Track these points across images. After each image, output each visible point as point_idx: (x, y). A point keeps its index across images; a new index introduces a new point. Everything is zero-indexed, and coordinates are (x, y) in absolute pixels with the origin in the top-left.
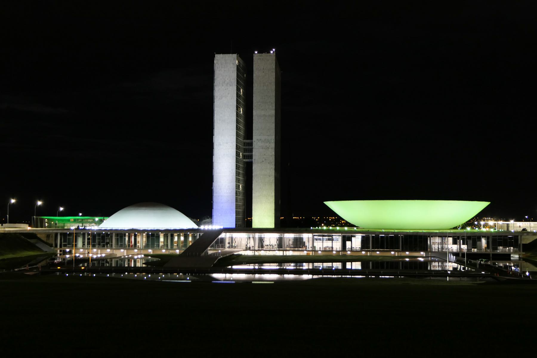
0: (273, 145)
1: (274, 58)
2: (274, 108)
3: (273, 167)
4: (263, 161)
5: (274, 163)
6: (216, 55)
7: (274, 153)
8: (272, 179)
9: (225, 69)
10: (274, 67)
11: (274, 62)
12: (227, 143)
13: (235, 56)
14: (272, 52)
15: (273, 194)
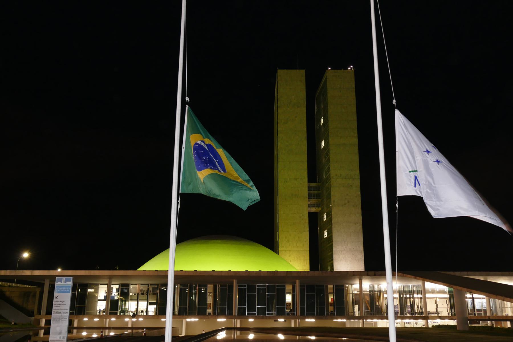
0: (357, 182)
1: (353, 74)
2: (356, 135)
3: (360, 211)
4: (345, 204)
5: (360, 207)
6: (279, 71)
7: (359, 193)
8: (359, 227)
9: (290, 88)
10: (354, 86)
11: (354, 80)
12: (295, 179)
13: (303, 72)
14: (349, 68)
15: (362, 248)
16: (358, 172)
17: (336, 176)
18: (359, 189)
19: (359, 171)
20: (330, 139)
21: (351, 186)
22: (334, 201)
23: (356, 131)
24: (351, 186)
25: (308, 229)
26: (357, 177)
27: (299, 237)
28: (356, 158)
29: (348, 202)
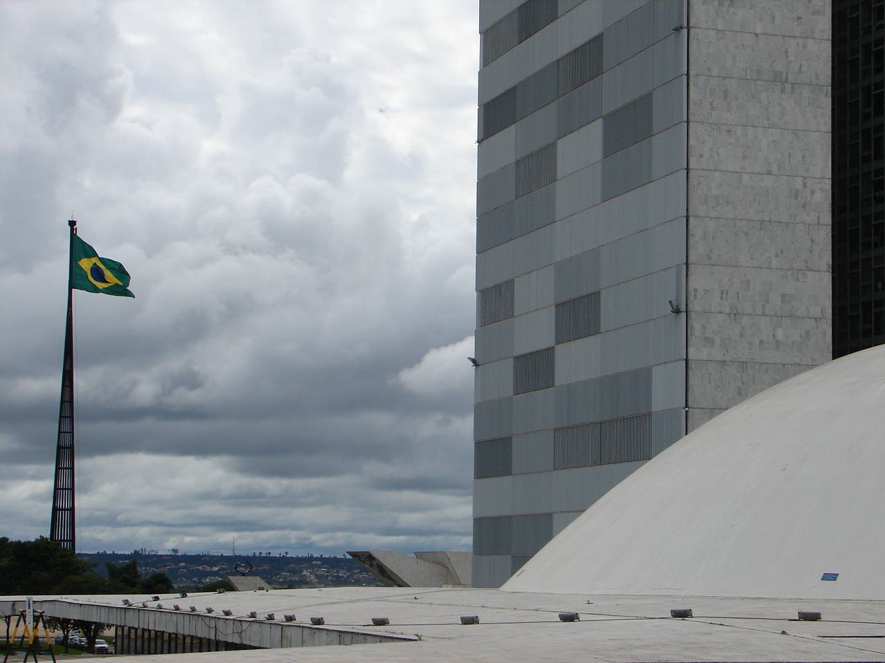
25: (827, 258)
27: (783, 296)
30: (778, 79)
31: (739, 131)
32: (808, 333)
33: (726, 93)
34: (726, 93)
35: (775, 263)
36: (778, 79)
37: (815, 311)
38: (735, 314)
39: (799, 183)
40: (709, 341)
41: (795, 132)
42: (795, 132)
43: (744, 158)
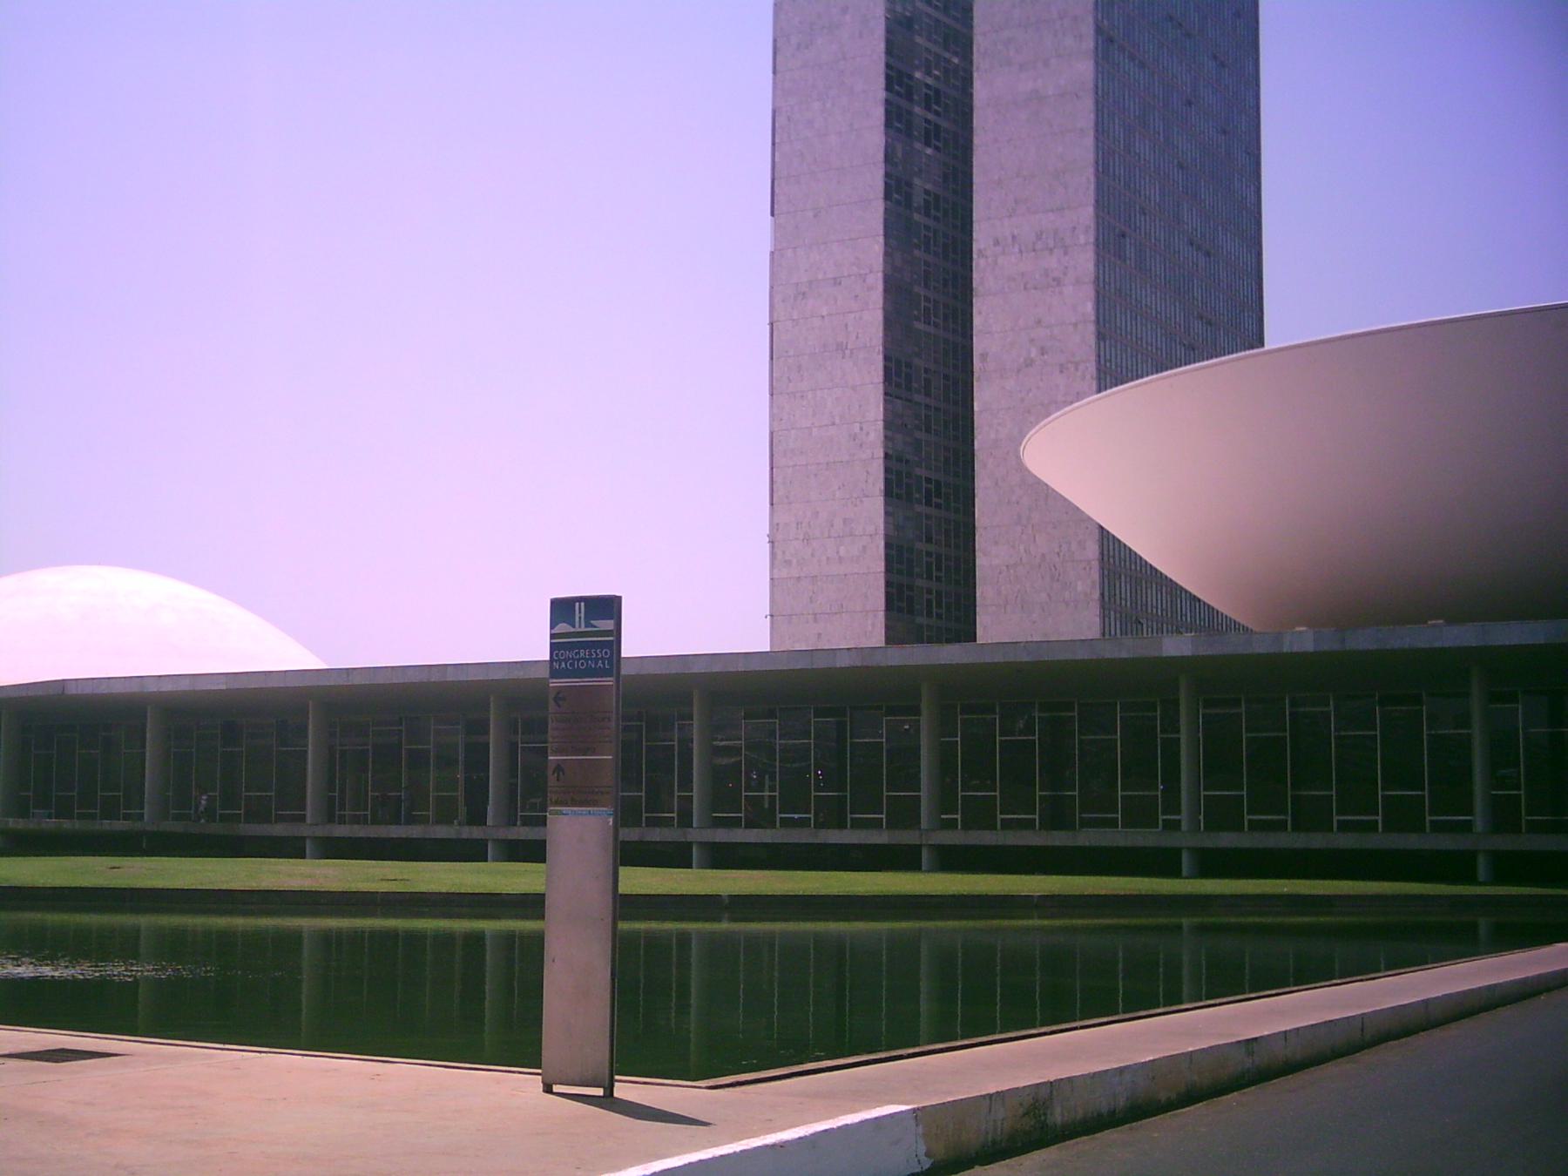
0: (1084, 261)
4: (1029, 363)
7: (1089, 307)
12: (836, 282)
16: (1087, 214)
17: (997, 243)
18: (1089, 291)
19: (1091, 210)
20: (977, 84)
21: (1058, 281)
22: (984, 356)
23: (1088, 28)
24: (1058, 281)
25: (881, 485)
26: (1082, 239)
27: (845, 521)
28: (1083, 150)
29: (1043, 351)
30: (841, 348)
31: (810, 395)
32: (864, 547)
33: (800, 367)
34: (800, 367)
35: (838, 494)
36: (841, 348)
37: (871, 529)
38: (807, 539)
39: (857, 430)
40: (788, 563)
41: (854, 388)
42: (854, 388)
43: (814, 415)
